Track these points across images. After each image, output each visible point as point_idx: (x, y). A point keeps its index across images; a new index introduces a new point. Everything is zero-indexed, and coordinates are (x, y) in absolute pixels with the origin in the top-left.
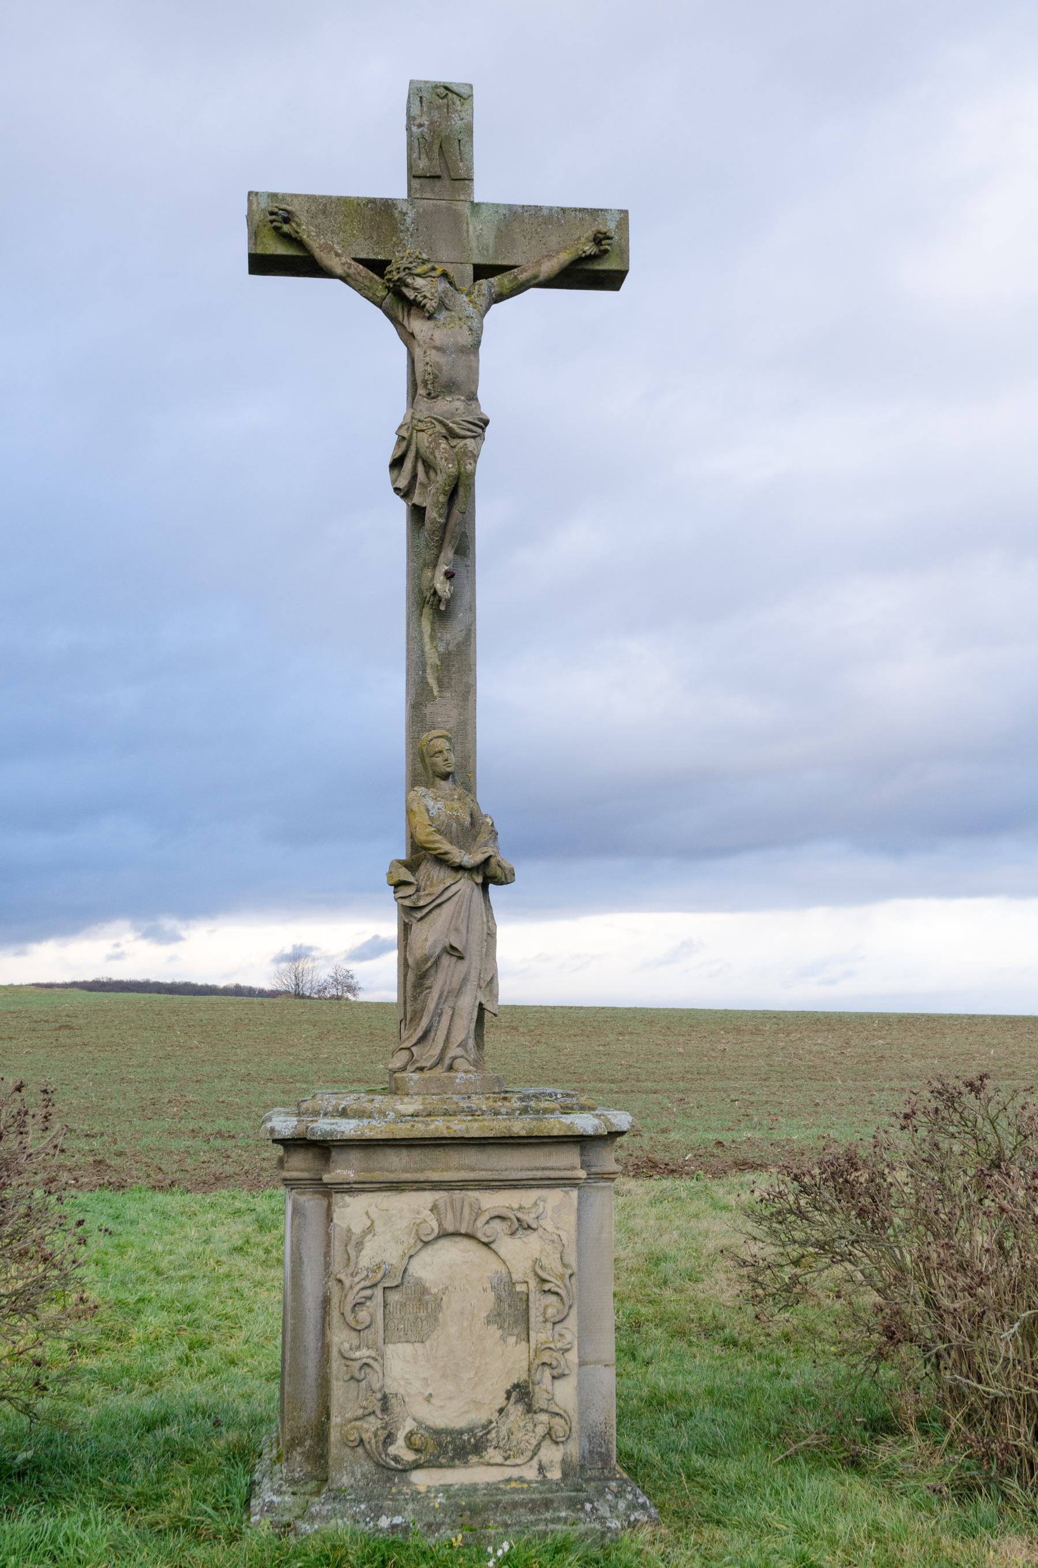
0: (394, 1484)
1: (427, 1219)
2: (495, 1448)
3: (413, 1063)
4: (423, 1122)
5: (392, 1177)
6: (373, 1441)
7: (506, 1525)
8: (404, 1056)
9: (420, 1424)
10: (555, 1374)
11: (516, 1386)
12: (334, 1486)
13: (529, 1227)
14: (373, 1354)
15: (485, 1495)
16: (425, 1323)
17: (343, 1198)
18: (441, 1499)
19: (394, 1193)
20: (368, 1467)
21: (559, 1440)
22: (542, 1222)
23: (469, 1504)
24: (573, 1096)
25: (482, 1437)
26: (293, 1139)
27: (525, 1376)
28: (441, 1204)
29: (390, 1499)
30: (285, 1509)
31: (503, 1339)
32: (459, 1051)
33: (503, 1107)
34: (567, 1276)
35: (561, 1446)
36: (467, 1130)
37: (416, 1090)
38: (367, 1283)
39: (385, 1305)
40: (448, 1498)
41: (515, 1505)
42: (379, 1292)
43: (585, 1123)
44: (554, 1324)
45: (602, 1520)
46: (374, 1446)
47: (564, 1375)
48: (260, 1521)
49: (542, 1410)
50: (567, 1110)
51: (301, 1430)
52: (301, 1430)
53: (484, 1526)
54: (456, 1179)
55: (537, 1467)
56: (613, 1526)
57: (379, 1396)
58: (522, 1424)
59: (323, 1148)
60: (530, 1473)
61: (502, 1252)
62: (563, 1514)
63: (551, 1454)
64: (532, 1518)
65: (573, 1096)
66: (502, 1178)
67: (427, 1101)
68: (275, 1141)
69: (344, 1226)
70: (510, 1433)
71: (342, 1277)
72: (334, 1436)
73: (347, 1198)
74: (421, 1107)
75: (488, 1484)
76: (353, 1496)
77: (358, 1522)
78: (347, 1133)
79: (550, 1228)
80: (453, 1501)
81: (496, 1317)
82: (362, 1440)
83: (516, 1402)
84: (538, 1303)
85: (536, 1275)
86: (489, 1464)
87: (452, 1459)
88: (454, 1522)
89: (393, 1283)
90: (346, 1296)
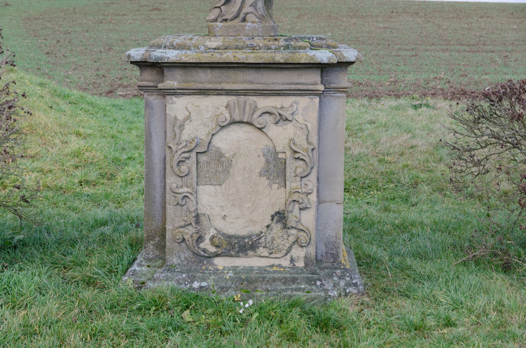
0: (204, 264)
1: (224, 113)
2: (264, 247)
3: (222, 16)
4: (220, 53)
5: (200, 86)
6: (190, 240)
7: (268, 291)
8: (217, 12)
9: (218, 231)
10: (301, 207)
11: (278, 213)
12: (169, 264)
13: (287, 119)
14: (190, 191)
15: (257, 273)
16: (221, 174)
17: (171, 98)
18: (231, 274)
19: (203, 96)
20: (188, 254)
21: (302, 245)
22: (295, 117)
23: (247, 278)
24: (324, 39)
25: (256, 241)
26: (142, 62)
27: (283, 208)
28: (231, 104)
29: (201, 273)
30: (143, 274)
31: (270, 185)
32: (250, 9)
33: (273, 45)
34: (310, 150)
35: (304, 249)
36: (247, 58)
37: (220, 33)
38: (186, 149)
39: (198, 163)
40: (235, 274)
41: (274, 280)
42: (193, 155)
43: (323, 56)
44: (302, 178)
45: (326, 291)
46: (191, 242)
47: (307, 208)
48: (127, 280)
49: (292, 227)
50: (313, 47)
51: (153, 232)
52: (153, 232)
53: (255, 290)
54: (240, 89)
55: (290, 259)
56: (332, 294)
57: (194, 214)
58: (280, 235)
59: (159, 67)
60: (286, 262)
61: (270, 134)
62: (303, 286)
63: (298, 253)
64: (284, 287)
65: (324, 39)
66: (270, 89)
67: (226, 40)
68: (132, 63)
69: (173, 115)
70: (273, 239)
71: (171, 145)
72: (168, 236)
73: (174, 99)
74: (221, 44)
75: (260, 267)
76: (179, 270)
77: (181, 284)
78: (171, 58)
79: (301, 120)
80: (237, 276)
81: (265, 172)
82: (184, 240)
83: (277, 222)
84: (292, 166)
85: (291, 148)
86: (260, 256)
87: (238, 252)
88: (237, 287)
89: (202, 150)
90: (173, 157)
